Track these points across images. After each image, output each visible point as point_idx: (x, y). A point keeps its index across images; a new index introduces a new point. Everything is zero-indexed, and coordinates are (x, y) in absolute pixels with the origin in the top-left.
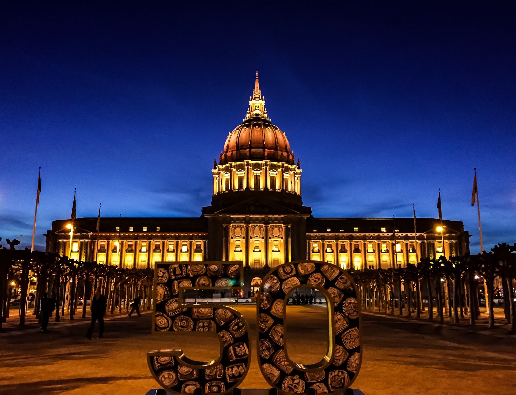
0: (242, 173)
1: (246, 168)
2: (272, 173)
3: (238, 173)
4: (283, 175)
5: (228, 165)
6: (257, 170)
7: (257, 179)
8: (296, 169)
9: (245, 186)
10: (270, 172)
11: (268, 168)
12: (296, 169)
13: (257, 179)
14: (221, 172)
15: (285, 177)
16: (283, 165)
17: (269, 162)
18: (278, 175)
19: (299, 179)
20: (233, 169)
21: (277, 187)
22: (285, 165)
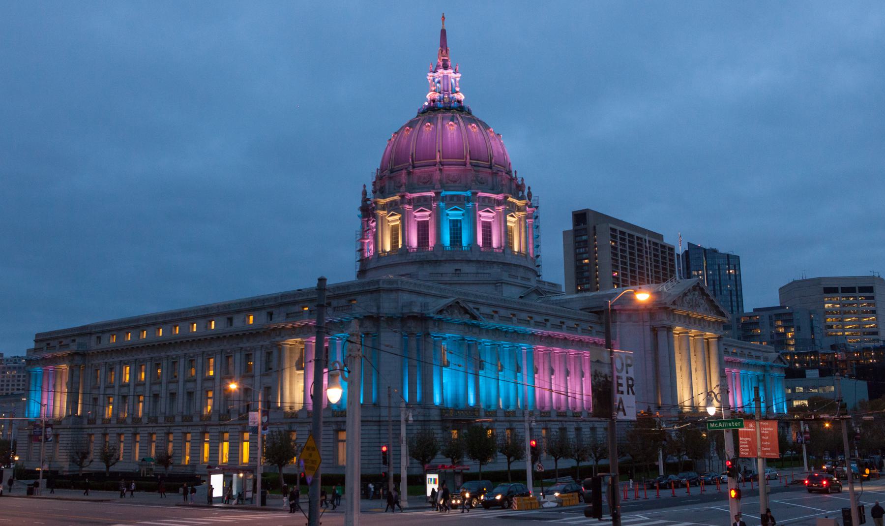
1: (434, 205)
2: (485, 216)
3: (417, 214)
4: (506, 221)
9: (432, 242)
10: (481, 213)
20: (407, 207)
21: (495, 244)
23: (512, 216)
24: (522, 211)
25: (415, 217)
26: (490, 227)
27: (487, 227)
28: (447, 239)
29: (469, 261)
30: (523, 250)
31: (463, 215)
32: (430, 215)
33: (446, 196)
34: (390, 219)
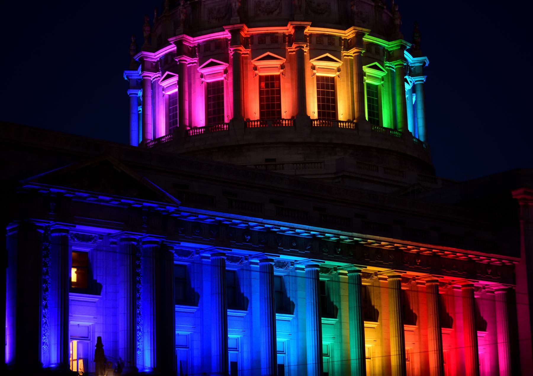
0: (215, 72)
1: (231, 51)
2: (322, 67)
4: (361, 75)
5: (172, 48)
6: (269, 58)
7: (270, 89)
8: (407, 55)
11: (306, 50)
12: (407, 55)
13: (270, 89)
14: (153, 76)
15: (367, 81)
16: (359, 35)
17: (309, 30)
18: (343, 72)
19: (419, 89)
20: (188, 60)
22: (367, 39)
23: (375, 67)
24: (396, 59)
25: (202, 76)
26: (334, 87)
27: (327, 89)
28: (254, 110)
29: (291, 144)
30: (400, 125)
31: (282, 67)
32: (226, 71)
33: (252, 36)
34: (165, 84)
